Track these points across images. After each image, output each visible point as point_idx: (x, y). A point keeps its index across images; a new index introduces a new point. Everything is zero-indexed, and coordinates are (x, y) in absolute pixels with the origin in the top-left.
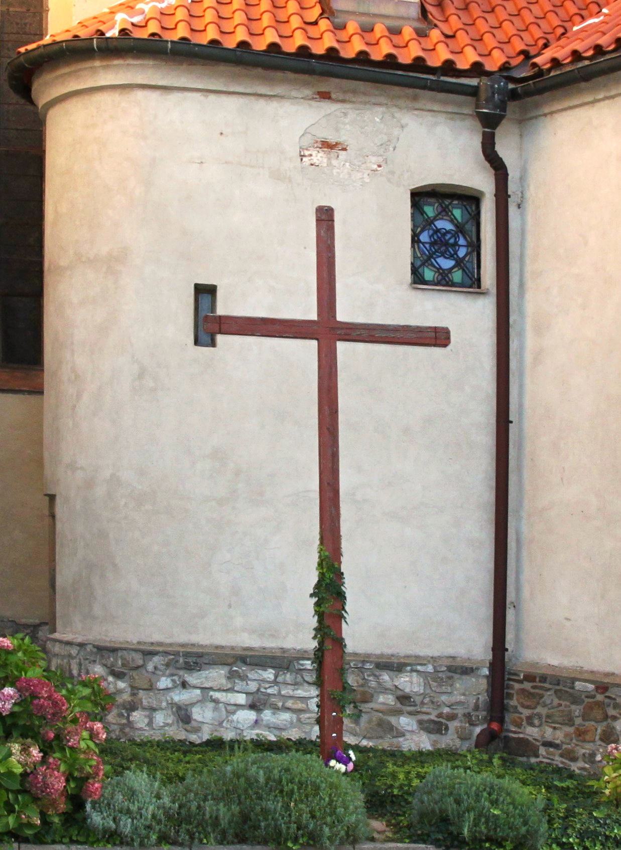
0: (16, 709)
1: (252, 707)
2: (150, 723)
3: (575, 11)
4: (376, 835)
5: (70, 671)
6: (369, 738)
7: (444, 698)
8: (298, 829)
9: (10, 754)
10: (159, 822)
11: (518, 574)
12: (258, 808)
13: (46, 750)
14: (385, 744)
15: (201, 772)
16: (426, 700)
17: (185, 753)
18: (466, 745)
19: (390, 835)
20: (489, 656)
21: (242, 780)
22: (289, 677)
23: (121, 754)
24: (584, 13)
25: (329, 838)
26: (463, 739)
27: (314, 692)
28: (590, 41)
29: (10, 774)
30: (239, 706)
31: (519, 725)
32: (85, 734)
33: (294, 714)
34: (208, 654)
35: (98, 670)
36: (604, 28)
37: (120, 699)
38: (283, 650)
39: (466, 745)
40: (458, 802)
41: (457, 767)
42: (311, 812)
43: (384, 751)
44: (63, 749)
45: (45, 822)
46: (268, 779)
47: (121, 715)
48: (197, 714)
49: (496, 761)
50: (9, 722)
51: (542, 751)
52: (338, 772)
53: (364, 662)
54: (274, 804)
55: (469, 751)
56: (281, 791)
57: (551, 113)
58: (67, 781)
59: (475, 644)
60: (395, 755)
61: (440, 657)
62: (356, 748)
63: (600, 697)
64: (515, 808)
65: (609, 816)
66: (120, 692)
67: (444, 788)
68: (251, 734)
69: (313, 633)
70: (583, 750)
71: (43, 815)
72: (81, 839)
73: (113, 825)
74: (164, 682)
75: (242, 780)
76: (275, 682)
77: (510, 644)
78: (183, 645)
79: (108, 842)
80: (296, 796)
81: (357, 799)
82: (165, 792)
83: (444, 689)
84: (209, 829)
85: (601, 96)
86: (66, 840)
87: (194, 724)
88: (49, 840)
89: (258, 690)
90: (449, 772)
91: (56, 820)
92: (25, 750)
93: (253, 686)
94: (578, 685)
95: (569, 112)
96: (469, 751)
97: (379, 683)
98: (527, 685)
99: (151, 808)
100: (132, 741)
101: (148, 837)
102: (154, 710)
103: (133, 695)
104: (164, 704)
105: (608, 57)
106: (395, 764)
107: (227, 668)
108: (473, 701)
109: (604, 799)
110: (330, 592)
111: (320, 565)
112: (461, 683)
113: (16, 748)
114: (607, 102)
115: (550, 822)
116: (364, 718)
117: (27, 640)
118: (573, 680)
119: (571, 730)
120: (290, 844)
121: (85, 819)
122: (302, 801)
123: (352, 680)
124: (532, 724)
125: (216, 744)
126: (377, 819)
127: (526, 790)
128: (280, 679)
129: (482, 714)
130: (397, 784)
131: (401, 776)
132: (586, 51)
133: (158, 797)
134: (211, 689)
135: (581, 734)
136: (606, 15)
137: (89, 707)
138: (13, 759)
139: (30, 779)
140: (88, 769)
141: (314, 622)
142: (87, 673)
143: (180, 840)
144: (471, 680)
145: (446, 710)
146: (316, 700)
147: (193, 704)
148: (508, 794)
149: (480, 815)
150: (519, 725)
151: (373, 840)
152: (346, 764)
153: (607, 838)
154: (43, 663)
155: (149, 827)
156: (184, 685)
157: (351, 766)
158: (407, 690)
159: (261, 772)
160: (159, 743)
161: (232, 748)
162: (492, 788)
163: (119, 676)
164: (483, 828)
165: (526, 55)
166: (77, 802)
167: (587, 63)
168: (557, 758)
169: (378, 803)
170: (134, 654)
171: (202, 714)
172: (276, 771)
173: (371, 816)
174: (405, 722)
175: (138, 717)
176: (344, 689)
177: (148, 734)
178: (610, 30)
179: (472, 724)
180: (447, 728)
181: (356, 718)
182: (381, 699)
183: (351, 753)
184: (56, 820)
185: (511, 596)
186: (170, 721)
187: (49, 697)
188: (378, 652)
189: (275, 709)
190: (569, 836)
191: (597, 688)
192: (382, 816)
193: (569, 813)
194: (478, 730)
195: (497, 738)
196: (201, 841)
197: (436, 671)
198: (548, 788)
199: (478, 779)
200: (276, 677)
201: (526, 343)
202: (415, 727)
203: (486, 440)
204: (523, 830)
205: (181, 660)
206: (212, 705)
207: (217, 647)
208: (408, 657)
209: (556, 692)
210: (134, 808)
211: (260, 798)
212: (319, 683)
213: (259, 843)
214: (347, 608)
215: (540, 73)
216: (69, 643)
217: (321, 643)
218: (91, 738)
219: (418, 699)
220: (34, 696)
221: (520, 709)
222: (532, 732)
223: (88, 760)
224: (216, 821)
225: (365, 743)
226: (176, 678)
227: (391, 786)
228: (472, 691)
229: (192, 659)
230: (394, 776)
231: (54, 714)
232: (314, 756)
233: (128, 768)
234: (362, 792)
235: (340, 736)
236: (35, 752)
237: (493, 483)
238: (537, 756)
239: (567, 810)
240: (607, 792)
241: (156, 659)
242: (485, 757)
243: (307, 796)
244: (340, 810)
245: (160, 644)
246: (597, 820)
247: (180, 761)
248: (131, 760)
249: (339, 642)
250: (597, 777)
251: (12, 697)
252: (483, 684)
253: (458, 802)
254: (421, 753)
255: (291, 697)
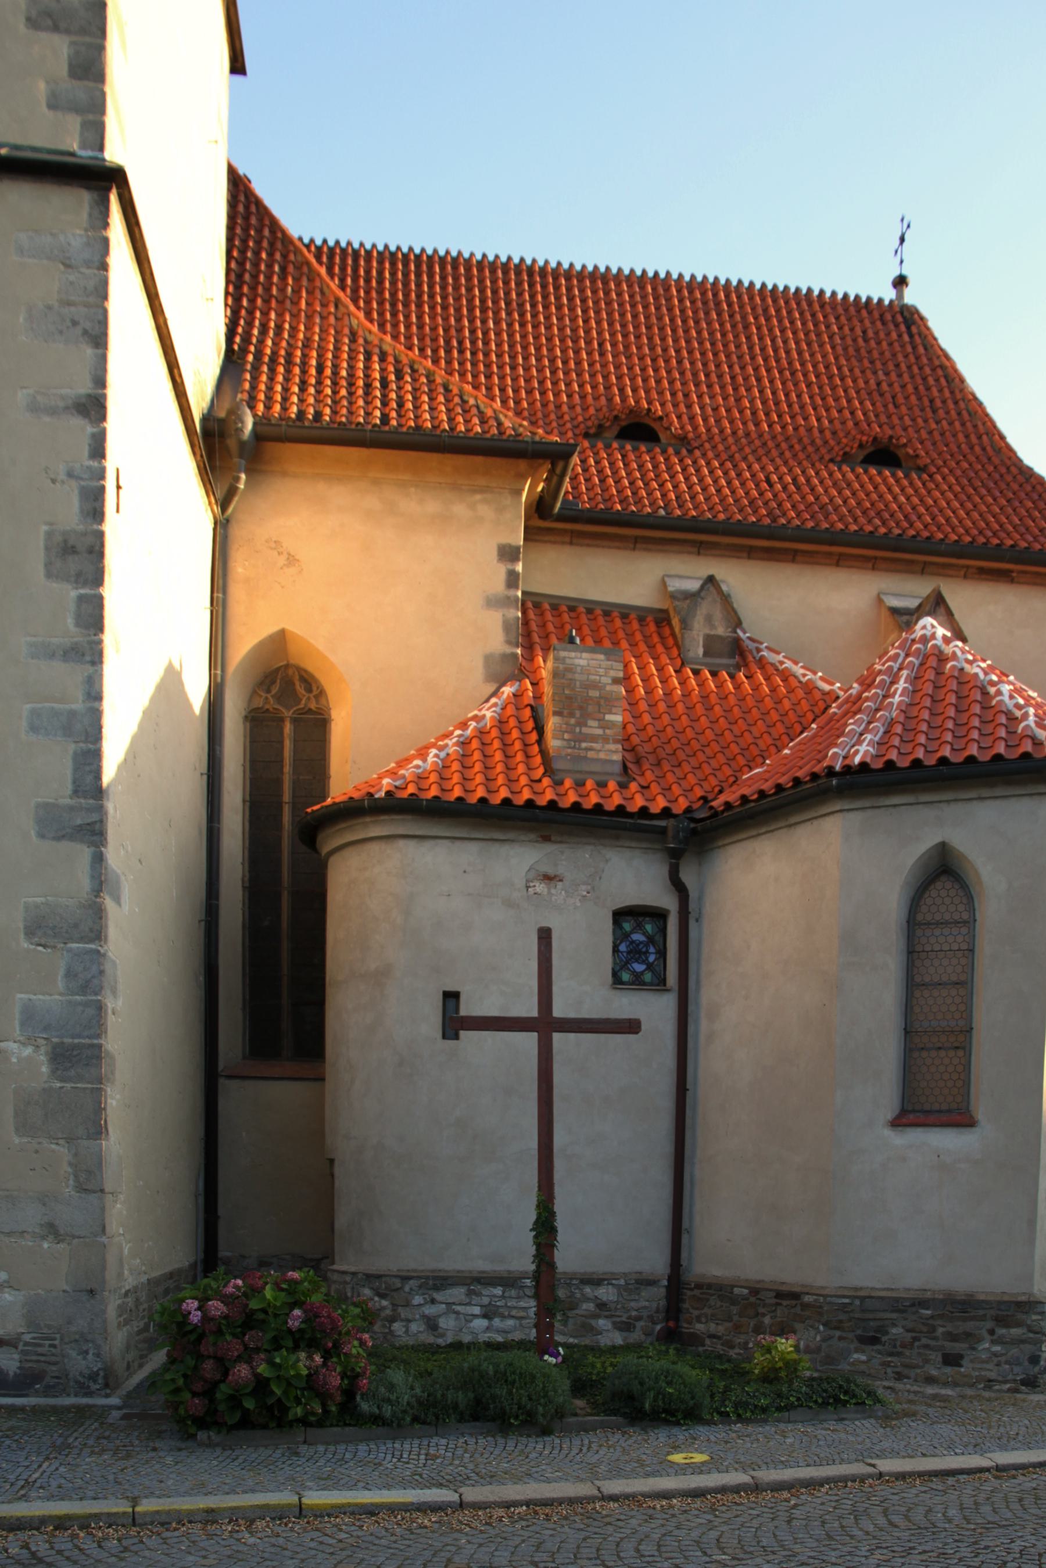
0: (303, 1326)
1: (485, 1316)
2: (407, 1332)
3: (745, 762)
4: (579, 1411)
5: (346, 1293)
6: (574, 1337)
7: (633, 1304)
8: (519, 1408)
9: (298, 1360)
10: (412, 1408)
11: (691, 1206)
12: (488, 1395)
13: (327, 1355)
14: (587, 1341)
15: (445, 1368)
16: (619, 1306)
17: (433, 1354)
18: (649, 1339)
19: (589, 1410)
20: (668, 1271)
21: (476, 1373)
22: (513, 1293)
23: (382, 1356)
24: (751, 764)
25: (543, 1415)
26: (647, 1335)
27: (533, 1303)
28: (756, 787)
29: (298, 1376)
30: (475, 1316)
31: (690, 1323)
32: (356, 1343)
33: (518, 1322)
34: (452, 1277)
35: (367, 1292)
36: (767, 776)
37: (383, 1314)
38: (509, 1272)
39: (649, 1339)
40: (642, 1384)
41: (642, 1357)
42: (528, 1396)
43: (586, 1346)
44: (339, 1356)
45: (326, 1411)
46: (496, 1372)
47: (384, 1326)
48: (442, 1323)
49: (671, 1351)
50: (297, 1336)
51: (708, 1342)
52: (550, 1364)
53: (571, 1279)
54: (501, 1391)
55: (651, 1344)
56: (506, 1381)
57: (724, 845)
58: (342, 1379)
59: (655, 1261)
60: (595, 1350)
61: (630, 1273)
62: (565, 1345)
63: (752, 1299)
64: (685, 1387)
65: (757, 1390)
66: (384, 1308)
67: (631, 1374)
68: (484, 1337)
69: (532, 1259)
70: (740, 1339)
71: (324, 1406)
72: (353, 1422)
73: (377, 1411)
74: (417, 1300)
75: (476, 1373)
76: (503, 1297)
77: (684, 1262)
78: (433, 1271)
79: (373, 1424)
80: (517, 1385)
81: (566, 1384)
82: (417, 1385)
83: (633, 1297)
84: (451, 1411)
85: (763, 830)
86: (341, 1423)
87: (440, 1331)
88: (328, 1424)
89: (490, 1303)
90: (635, 1361)
91: (334, 1409)
92: (310, 1357)
93: (486, 1301)
94: (736, 1290)
95: (738, 845)
96: (651, 1344)
97: (583, 1295)
98: (697, 1292)
99: (406, 1397)
100: (393, 1347)
101: (403, 1419)
102: (409, 1321)
103: (394, 1310)
104: (418, 1316)
105: (769, 799)
106: (594, 1356)
107: (466, 1287)
108: (655, 1305)
109: (754, 1377)
110: (545, 1227)
111: (538, 1206)
112: (646, 1293)
113: (303, 1355)
114: (768, 835)
115: (712, 1396)
116: (571, 1321)
117: (312, 1273)
118: (733, 1287)
119: (729, 1325)
120: (512, 1421)
121: (356, 1407)
122: (521, 1388)
123: (561, 1293)
124: (700, 1322)
125: (457, 1346)
126: (579, 1399)
127: (694, 1373)
128: (507, 1294)
129: (661, 1316)
130: (595, 1372)
131: (599, 1365)
132: (752, 795)
133: (412, 1388)
134: (454, 1303)
135: (737, 1327)
136: (768, 765)
137: (359, 1323)
138: (301, 1364)
139: (314, 1377)
140: (358, 1370)
141: (532, 1250)
142: (359, 1296)
143: (428, 1420)
144: (653, 1290)
145: (634, 1313)
146: (534, 1309)
147: (439, 1316)
148: (680, 1376)
149: (659, 1393)
150: (690, 1323)
151: (576, 1415)
152: (556, 1357)
153: (756, 1406)
154: (324, 1290)
155: (405, 1412)
156: (433, 1301)
157: (560, 1359)
158: (604, 1299)
159: (491, 1367)
160: (413, 1347)
161: (469, 1348)
162: (668, 1372)
163: (382, 1296)
164: (660, 1403)
165: (704, 799)
166: (349, 1394)
167: (752, 804)
168: (719, 1346)
169: (580, 1388)
170: (394, 1280)
171: (447, 1323)
172: (502, 1366)
173: (575, 1397)
174: (602, 1323)
175: (397, 1326)
176: (556, 1300)
177: (405, 1340)
178: (771, 778)
179: (654, 1323)
180: (635, 1327)
181: (565, 1322)
182: (585, 1306)
183: (561, 1349)
184: (334, 1409)
185: (685, 1224)
186: (421, 1329)
187: (329, 1316)
188: (582, 1271)
189: (503, 1317)
190: (726, 1406)
191: (750, 1292)
192: (583, 1396)
193: (727, 1389)
194: (658, 1327)
195: (673, 1334)
196: (444, 1420)
197: (627, 1284)
198: (711, 1370)
199: (658, 1365)
200: (504, 1292)
201: (702, 1027)
202: (610, 1326)
203: (667, 1104)
204: (692, 1402)
205: (431, 1282)
206: (454, 1316)
207: (458, 1272)
208: (605, 1273)
209: (719, 1296)
210: (393, 1397)
211: (490, 1387)
212: (537, 1296)
213: (488, 1421)
214: (558, 1238)
215: (715, 814)
216: (344, 1273)
217: (538, 1267)
218: (360, 1346)
219: (613, 1306)
220: (317, 1316)
221: (691, 1310)
222: (700, 1327)
223: (357, 1362)
224: (456, 1406)
225: (571, 1340)
226: (426, 1296)
227: (591, 1374)
228: (654, 1298)
229: (440, 1281)
230: (593, 1366)
231: (332, 1329)
232: (532, 1354)
233: (389, 1367)
234: (568, 1378)
235: (552, 1336)
236: (318, 1359)
237: (673, 1138)
238: (703, 1345)
239: (725, 1387)
240: (756, 1371)
241: (411, 1282)
242: (663, 1348)
243: (525, 1384)
244: (551, 1393)
245: (415, 1271)
246: (748, 1393)
247: (429, 1360)
248: (391, 1361)
249: (552, 1265)
250: (749, 1359)
251: (299, 1317)
252: (663, 1291)
253: (642, 1384)
254: (614, 1347)
255: (515, 1308)
